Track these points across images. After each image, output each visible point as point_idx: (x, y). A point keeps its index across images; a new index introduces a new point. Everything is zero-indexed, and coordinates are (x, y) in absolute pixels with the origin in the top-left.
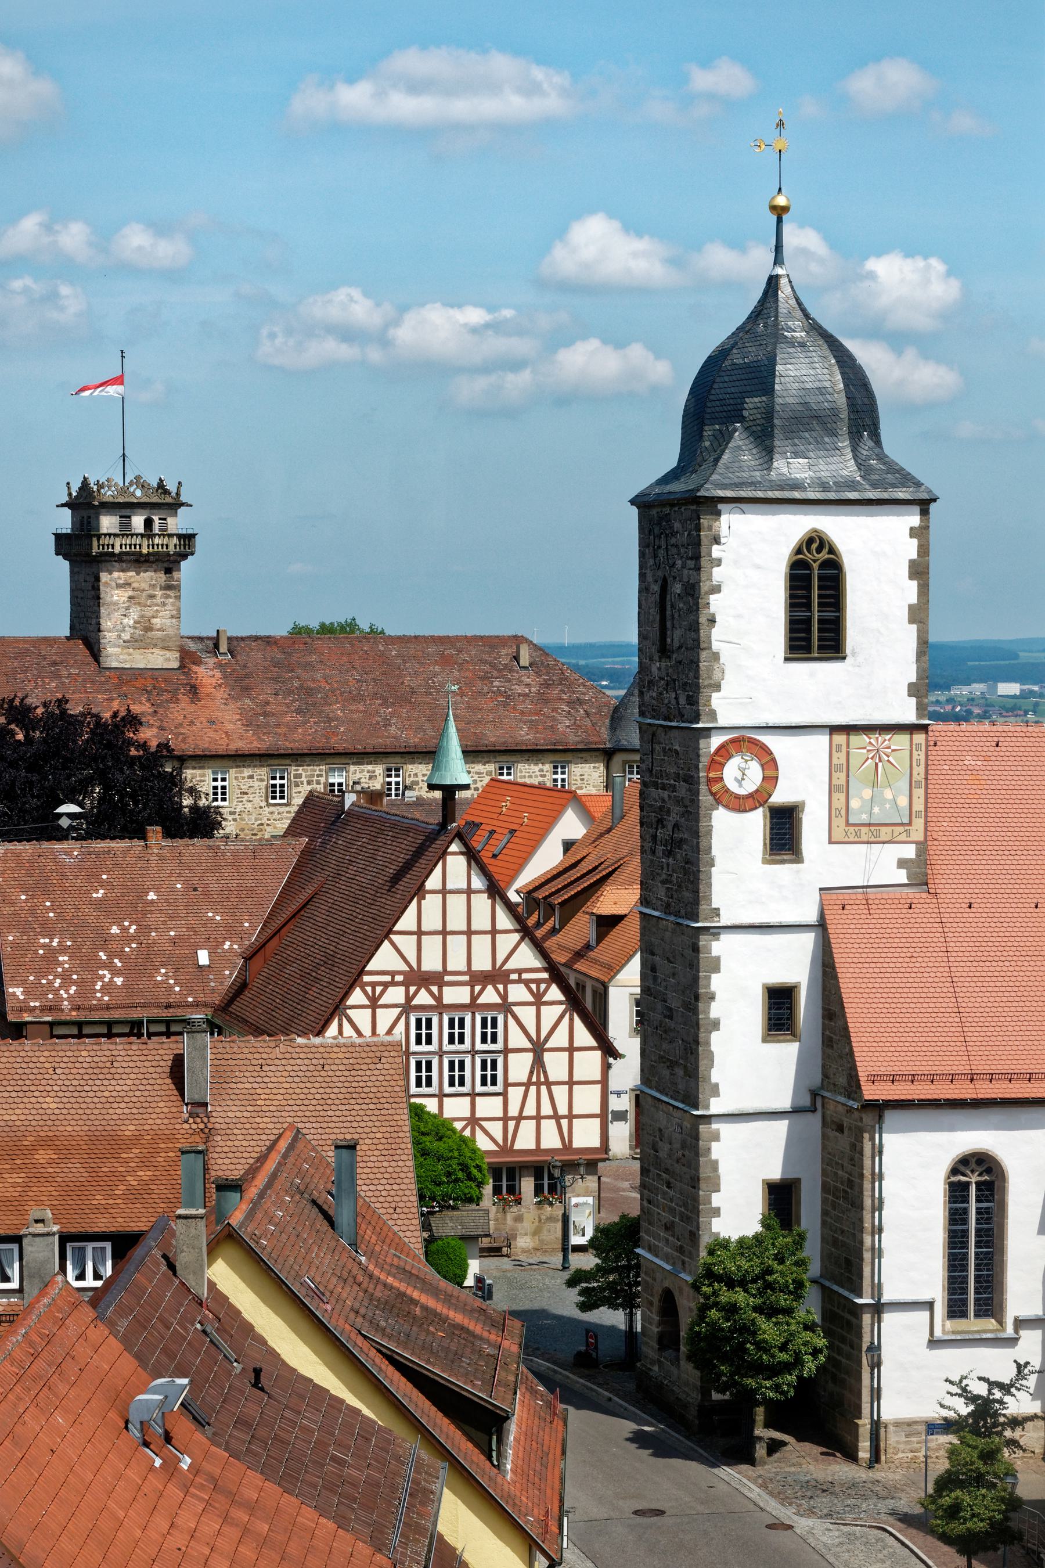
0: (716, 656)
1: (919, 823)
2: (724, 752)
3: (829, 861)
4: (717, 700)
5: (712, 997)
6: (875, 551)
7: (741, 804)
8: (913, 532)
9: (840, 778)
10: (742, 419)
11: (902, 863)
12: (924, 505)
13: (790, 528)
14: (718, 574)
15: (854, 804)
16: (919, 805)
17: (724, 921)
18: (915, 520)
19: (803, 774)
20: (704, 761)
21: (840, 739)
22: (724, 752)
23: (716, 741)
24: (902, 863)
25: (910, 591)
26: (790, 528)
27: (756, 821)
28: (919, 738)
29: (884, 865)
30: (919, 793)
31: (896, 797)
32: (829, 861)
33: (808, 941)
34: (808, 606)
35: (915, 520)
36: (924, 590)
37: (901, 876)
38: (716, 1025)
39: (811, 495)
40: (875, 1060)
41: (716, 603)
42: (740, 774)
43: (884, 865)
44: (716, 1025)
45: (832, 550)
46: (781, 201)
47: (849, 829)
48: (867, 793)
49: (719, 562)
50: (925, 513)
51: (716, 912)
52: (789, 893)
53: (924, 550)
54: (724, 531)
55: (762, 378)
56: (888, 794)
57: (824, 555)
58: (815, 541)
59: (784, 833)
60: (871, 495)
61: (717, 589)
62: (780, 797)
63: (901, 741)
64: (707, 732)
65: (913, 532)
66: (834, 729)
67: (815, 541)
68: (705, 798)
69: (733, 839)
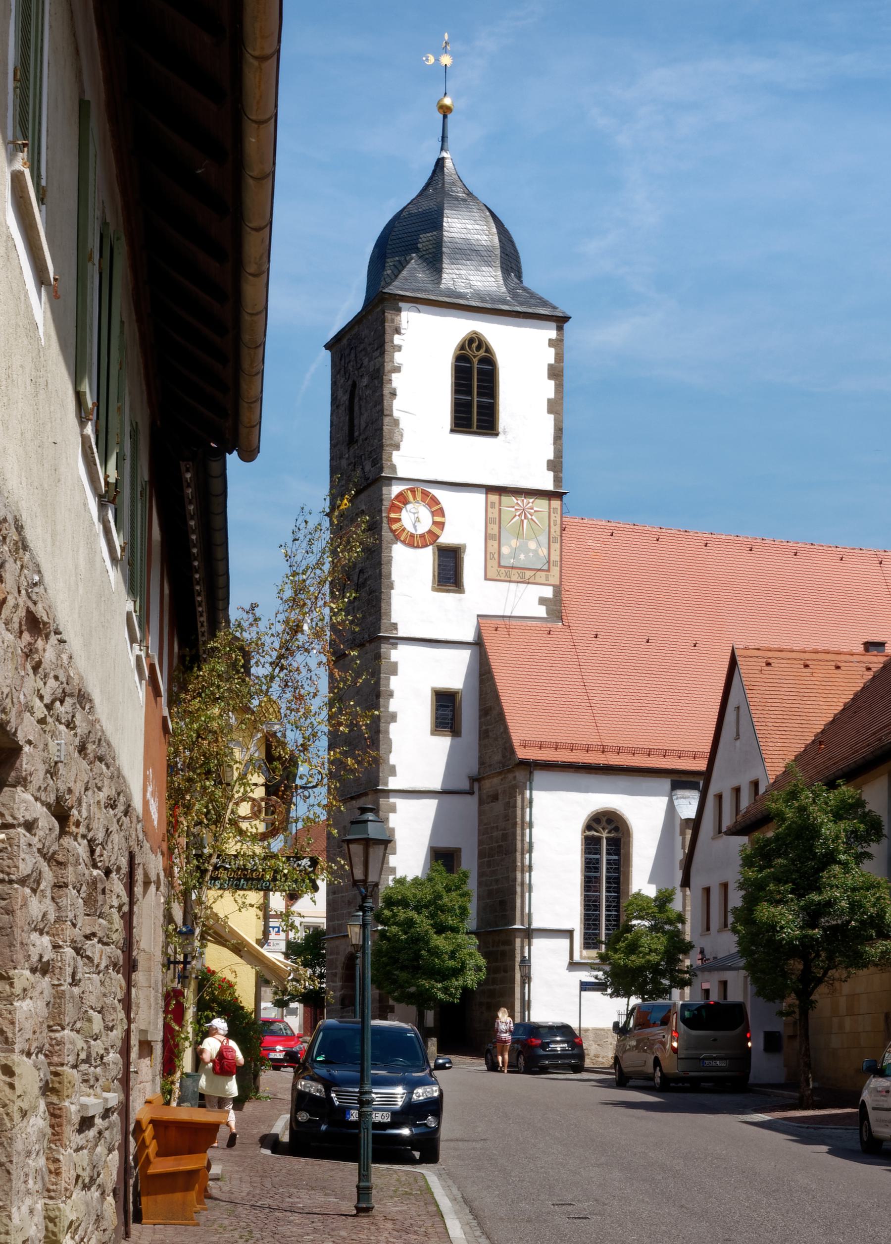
0: (396, 422)
1: (555, 570)
2: (402, 498)
3: (484, 595)
4: (397, 458)
5: (391, 694)
6: (522, 356)
7: (414, 542)
8: (551, 343)
9: (494, 529)
10: (417, 250)
11: (542, 601)
12: (561, 321)
13: (455, 329)
14: (398, 358)
15: (505, 550)
16: (555, 556)
17: (401, 634)
18: (553, 334)
19: (465, 522)
20: (386, 504)
21: (494, 498)
22: (402, 498)
23: (396, 489)
24: (542, 601)
25: (549, 389)
26: (455, 329)
27: (426, 558)
28: (556, 503)
29: (527, 601)
30: (556, 546)
31: (536, 549)
32: (484, 595)
33: (465, 655)
34: (469, 393)
35: (553, 334)
36: (559, 388)
37: (542, 612)
38: (393, 717)
39: (474, 304)
40: (526, 731)
41: (397, 381)
42: (414, 518)
43: (527, 601)
44: (393, 717)
45: (488, 350)
46: (447, 101)
47: (501, 570)
48: (514, 543)
49: (399, 348)
50: (560, 329)
51: (395, 626)
52: (454, 615)
53: (559, 357)
54: (404, 325)
55: (435, 222)
56: (532, 545)
57: (482, 353)
58: (474, 342)
59: (449, 571)
60: (519, 309)
61: (398, 369)
62: (447, 538)
63: (541, 505)
64: (390, 480)
65: (551, 343)
66: (490, 489)
67: (474, 342)
68: (386, 534)
69: (409, 572)
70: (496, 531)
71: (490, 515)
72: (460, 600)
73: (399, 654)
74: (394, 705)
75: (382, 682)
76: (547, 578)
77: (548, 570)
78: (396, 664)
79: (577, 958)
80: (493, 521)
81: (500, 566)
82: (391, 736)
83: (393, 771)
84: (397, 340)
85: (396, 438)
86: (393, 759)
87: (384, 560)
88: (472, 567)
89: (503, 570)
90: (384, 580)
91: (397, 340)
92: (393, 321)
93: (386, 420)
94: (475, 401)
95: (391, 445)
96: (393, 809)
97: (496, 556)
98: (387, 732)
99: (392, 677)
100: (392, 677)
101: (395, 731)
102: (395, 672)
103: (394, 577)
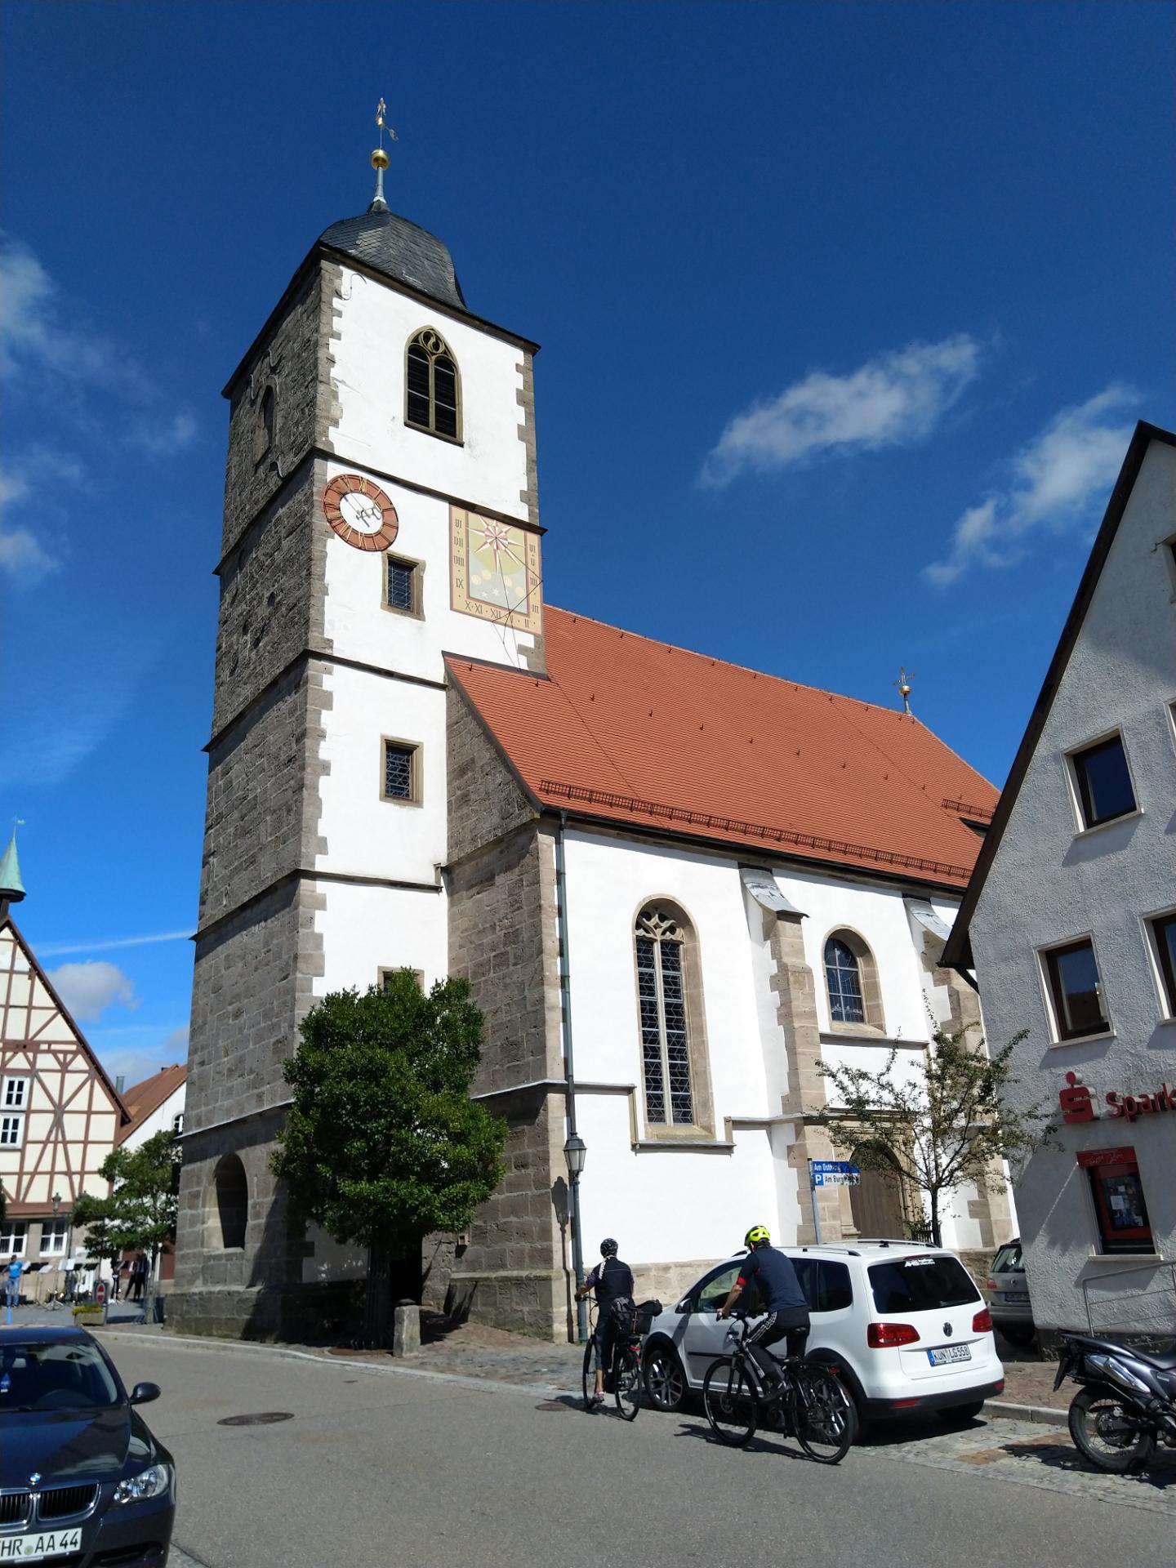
2: (340, 489)
5: (322, 735)
7: (356, 541)
11: (522, 650)
15: (474, 579)
19: (423, 532)
21: (460, 513)
24: (522, 650)
27: (375, 564)
29: (505, 646)
38: (325, 768)
44: (325, 768)
45: (447, 351)
49: (340, 314)
61: (337, 336)
69: (348, 584)
70: (463, 555)
71: (455, 534)
72: (420, 628)
73: (335, 680)
74: (325, 751)
75: (309, 716)
76: (527, 622)
77: (528, 615)
78: (330, 694)
79: (642, 1138)
80: (459, 542)
81: (469, 597)
82: (321, 794)
83: (322, 846)
84: (336, 303)
85: (334, 412)
86: (324, 828)
87: (316, 555)
88: (434, 587)
89: (473, 603)
90: (316, 585)
91: (336, 303)
92: (331, 281)
93: (321, 388)
94: (433, 397)
95: (327, 418)
96: (321, 904)
97: (464, 584)
98: (316, 788)
99: (324, 712)
100: (324, 712)
101: (327, 788)
102: (328, 705)
103: (329, 578)
